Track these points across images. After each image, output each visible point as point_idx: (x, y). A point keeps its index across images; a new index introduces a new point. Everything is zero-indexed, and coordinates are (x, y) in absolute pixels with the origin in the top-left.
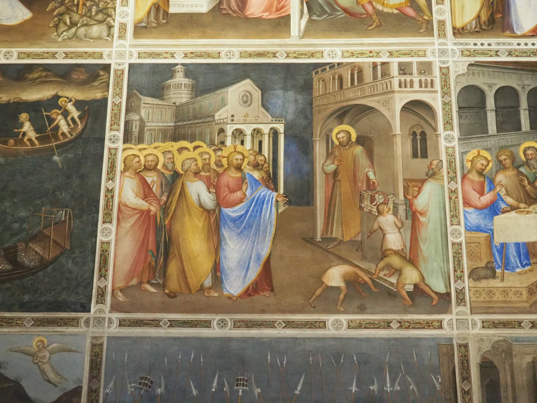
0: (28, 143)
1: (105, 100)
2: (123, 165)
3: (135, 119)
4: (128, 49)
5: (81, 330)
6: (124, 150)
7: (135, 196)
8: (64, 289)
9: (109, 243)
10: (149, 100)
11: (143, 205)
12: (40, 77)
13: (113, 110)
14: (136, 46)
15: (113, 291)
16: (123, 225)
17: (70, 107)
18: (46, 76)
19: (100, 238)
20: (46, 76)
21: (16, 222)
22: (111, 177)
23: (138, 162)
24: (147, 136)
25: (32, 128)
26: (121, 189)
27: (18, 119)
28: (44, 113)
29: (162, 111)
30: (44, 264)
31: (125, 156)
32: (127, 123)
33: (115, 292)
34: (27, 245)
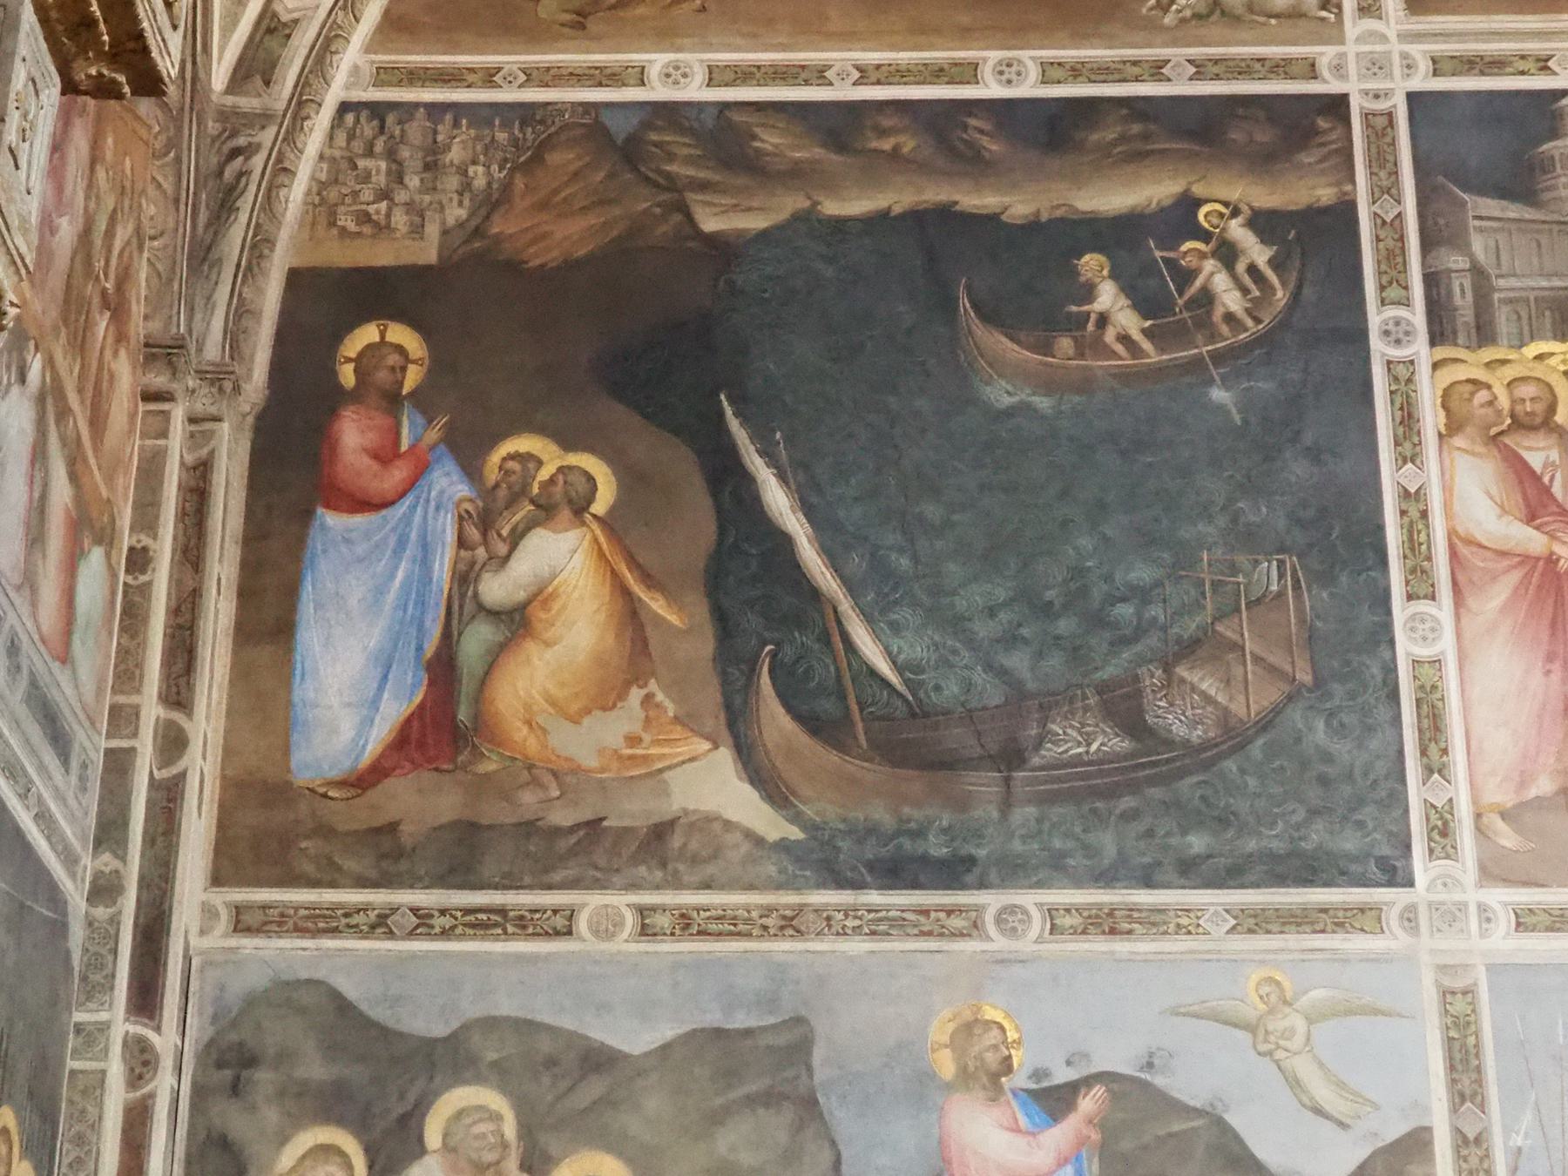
0: (1119, 348)
1: (1345, 211)
2: (1442, 414)
3: (1454, 266)
4: (1396, 47)
5: (1393, 944)
6: (1436, 366)
7: (1498, 511)
8: (1314, 813)
9: (1437, 663)
10: (1490, 206)
11: (1532, 540)
12: (1123, 139)
13: (1378, 240)
14: (1418, 37)
15: (1478, 816)
16: (1472, 602)
17: (1237, 231)
18: (1146, 137)
19: (1405, 647)
20: (1146, 137)
21: (1124, 600)
22: (1409, 454)
23: (1490, 403)
24: (1503, 320)
25: (1123, 301)
26: (1447, 489)
27: (1075, 273)
28: (1158, 254)
29: (1539, 245)
30: (1234, 736)
31: (1444, 385)
32: (1430, 280)
33: (1485, 820)
34: (1168, 669)
